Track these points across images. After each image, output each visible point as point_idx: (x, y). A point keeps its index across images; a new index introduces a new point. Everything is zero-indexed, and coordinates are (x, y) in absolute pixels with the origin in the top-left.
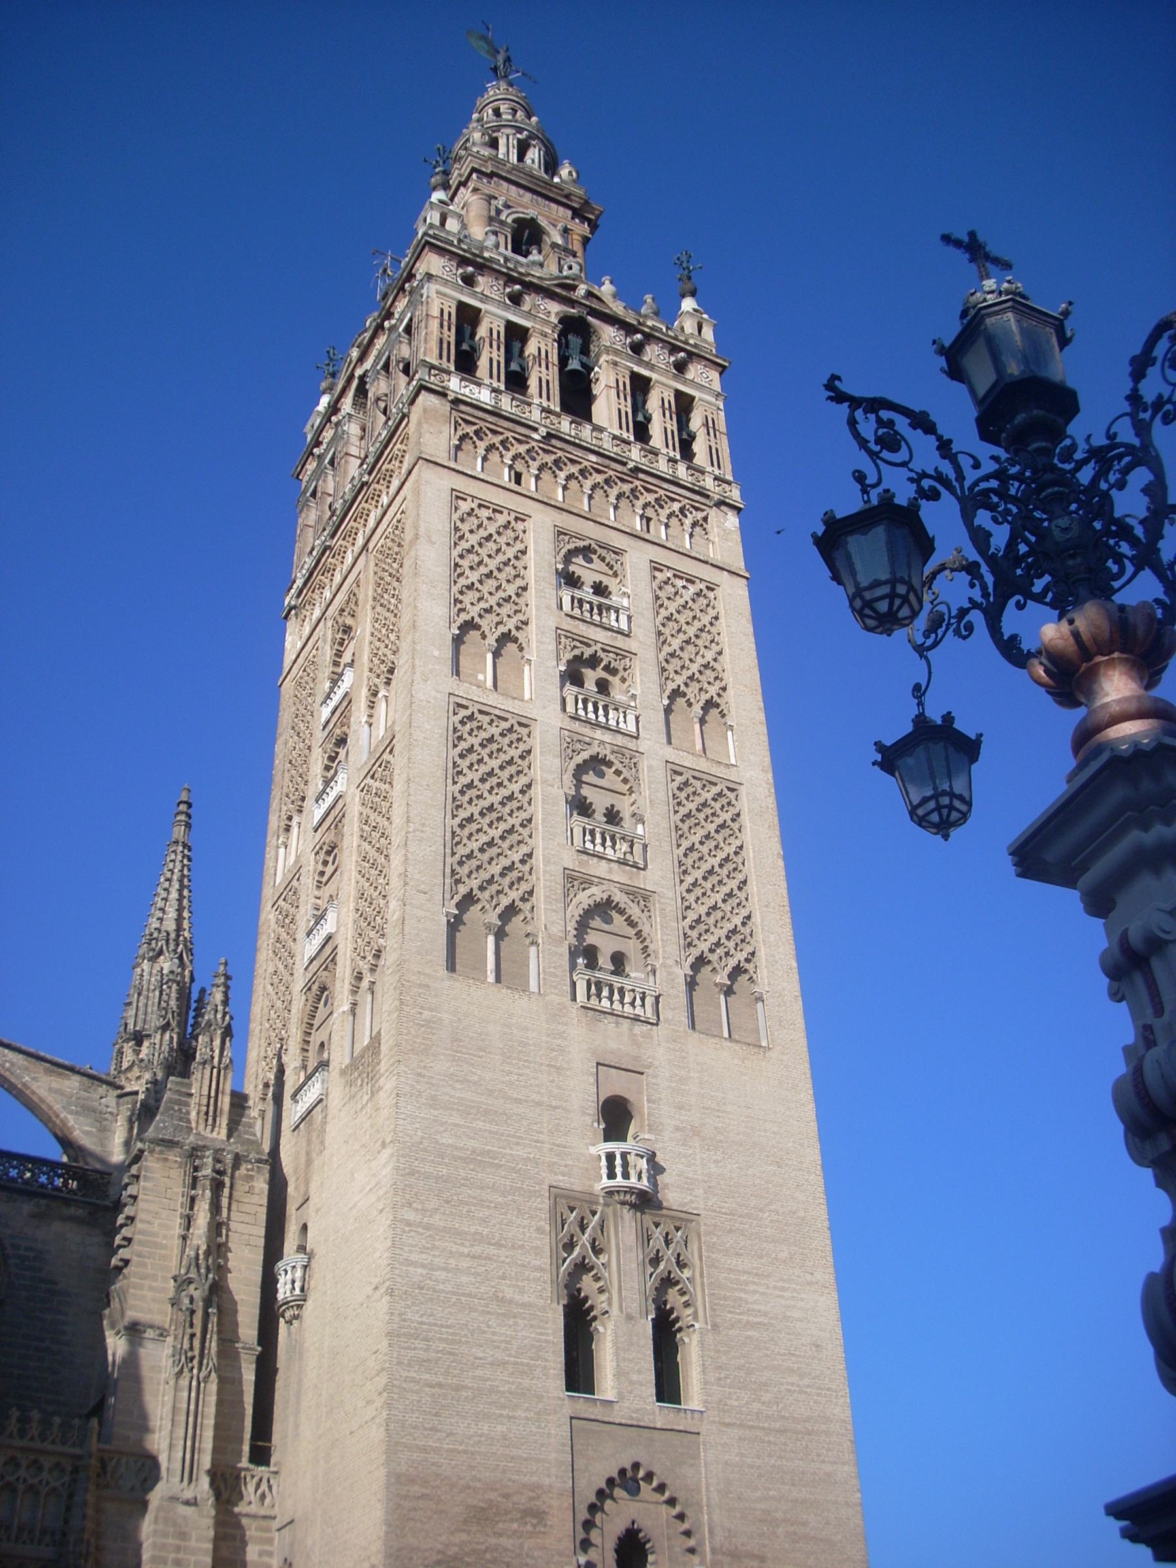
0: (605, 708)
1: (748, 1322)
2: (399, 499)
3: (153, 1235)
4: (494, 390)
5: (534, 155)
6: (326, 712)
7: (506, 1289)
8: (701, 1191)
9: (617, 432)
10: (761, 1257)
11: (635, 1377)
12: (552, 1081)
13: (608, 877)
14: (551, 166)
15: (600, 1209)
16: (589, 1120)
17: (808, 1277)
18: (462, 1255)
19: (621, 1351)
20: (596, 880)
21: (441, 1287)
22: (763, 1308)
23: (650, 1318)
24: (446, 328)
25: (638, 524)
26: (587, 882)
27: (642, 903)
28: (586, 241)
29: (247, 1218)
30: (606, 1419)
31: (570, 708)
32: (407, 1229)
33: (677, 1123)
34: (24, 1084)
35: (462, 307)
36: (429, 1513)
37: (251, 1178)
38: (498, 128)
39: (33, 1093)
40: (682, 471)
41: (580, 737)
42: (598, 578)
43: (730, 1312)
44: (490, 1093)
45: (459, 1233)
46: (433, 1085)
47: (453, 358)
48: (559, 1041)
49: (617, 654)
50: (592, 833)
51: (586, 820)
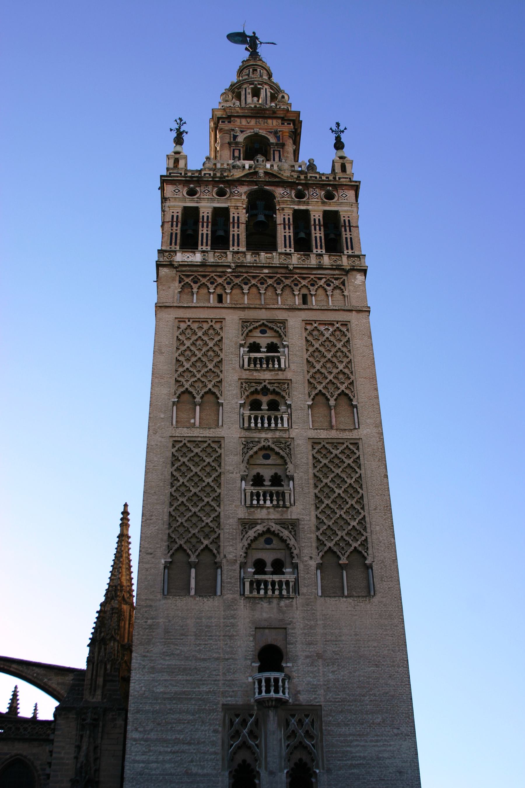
1: (351, 764)
4: (203, 252)
8: (322, 691)
10: (362, 724)
12: (227, 644)
16: (249, 662)
17: (395, 731)
18: (166, 752)
20: (259, 521)
21: (154, 772)
23: (285, 771)
24: (175, 226)
25: (298, 301)
26: (253, 524)
32: (134, 743)
33: (308, 653)
34: (45, 683)
39: (50, 687)
40: (326, 260)
41: (252, 440)
42: (269, 341)
44: (187, 658)
46: (152, 660)
47: (178, 241)
49: (279, 383)
50: (258, 495)
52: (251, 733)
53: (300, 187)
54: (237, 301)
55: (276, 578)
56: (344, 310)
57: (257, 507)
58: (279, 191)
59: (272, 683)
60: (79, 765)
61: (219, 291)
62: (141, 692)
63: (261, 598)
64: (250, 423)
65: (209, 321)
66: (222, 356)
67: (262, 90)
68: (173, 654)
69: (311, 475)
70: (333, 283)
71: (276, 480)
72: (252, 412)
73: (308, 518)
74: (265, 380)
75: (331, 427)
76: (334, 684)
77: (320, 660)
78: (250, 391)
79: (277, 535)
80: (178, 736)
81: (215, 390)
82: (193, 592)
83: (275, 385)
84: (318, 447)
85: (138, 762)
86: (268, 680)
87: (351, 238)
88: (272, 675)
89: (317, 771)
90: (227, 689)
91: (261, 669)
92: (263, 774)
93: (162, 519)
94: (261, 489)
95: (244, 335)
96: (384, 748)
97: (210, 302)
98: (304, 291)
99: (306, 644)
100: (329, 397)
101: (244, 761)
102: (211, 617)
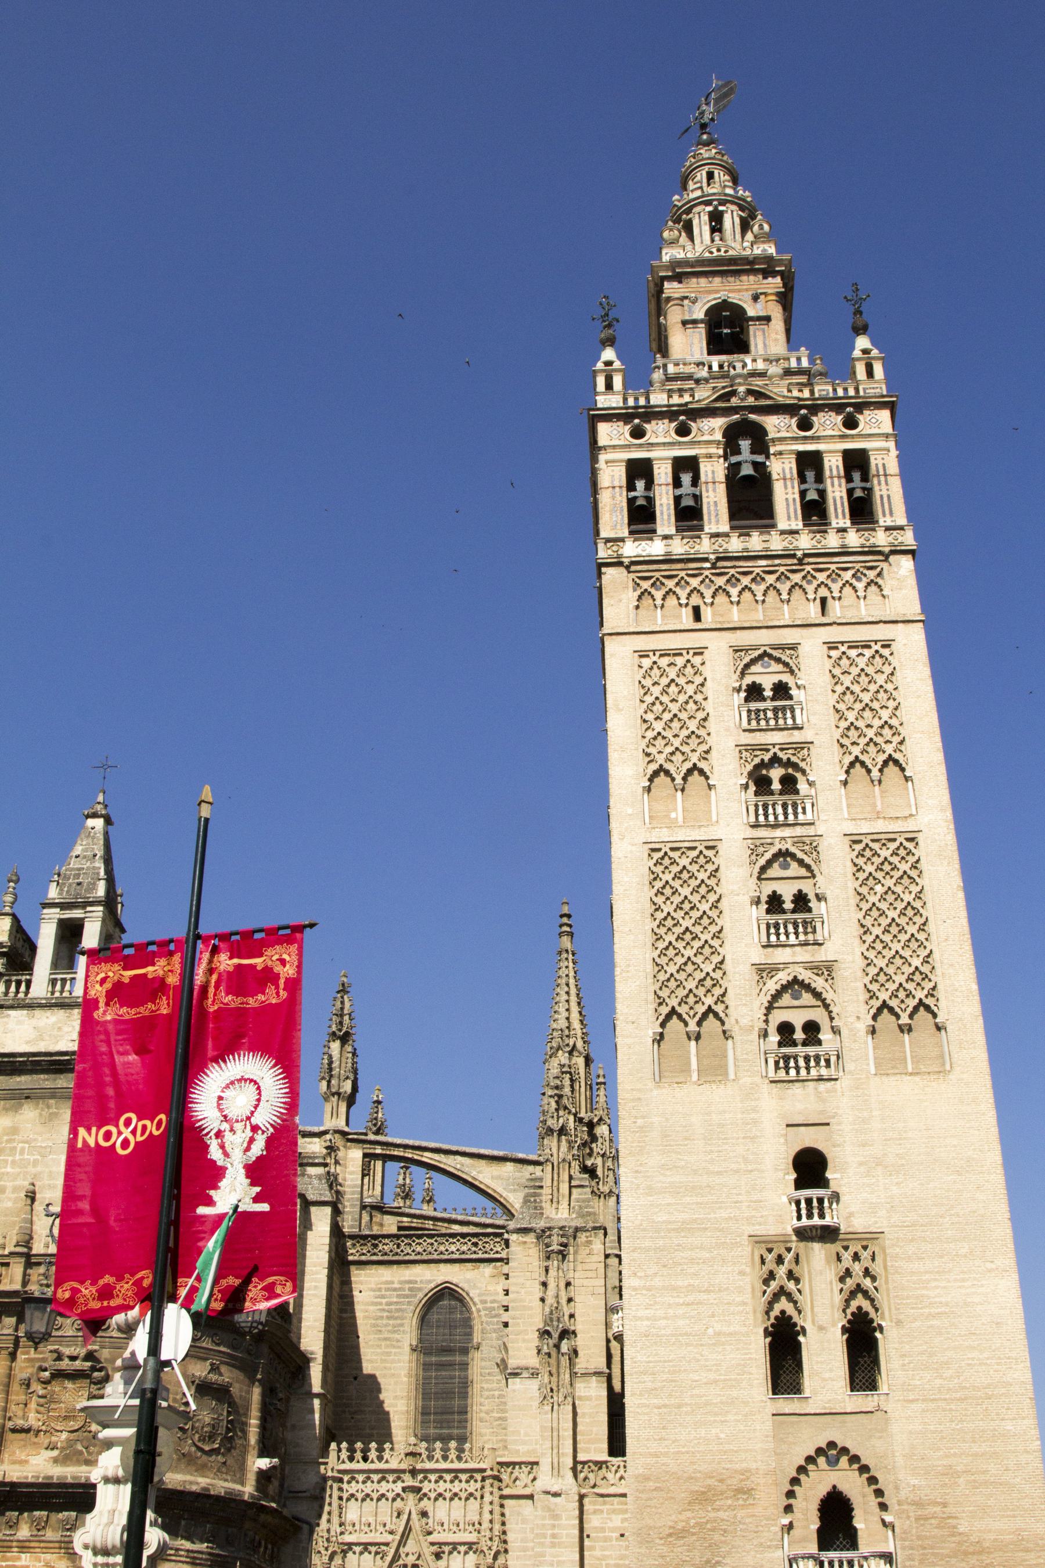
1: (930, 1314)
4: (666, 537)
7: (715, 1324)
8: (884, 1212)
10: (942, 1257)
11: (827, 1375)
13: (793, 959)
15: (793, 1245)
16: (781, 1174)
17: (989, 1265)
18: (678, 1304)
19: (824, 1354)
21: (663, 1332)
22: (943, 1300)
23: (840, 1325)
25: (813, 611)
26: (772, 970)
27: (826, 973)
29: (590, 1274)
30: (802, 1412)
33: (862, 1159)
36: (661, 1501)
37: (589, 1242)
41: (763, 841)
42: (776, 678)
43: (913, 1308)
44: (695, 1172)
45: (674, 1288)
46: (648, 1177)
48: (753, 1115)
49: (795, 749)
50: (777, 926)
51: (768, 917)
52: (790, 1275)
53: (803, 412)
54: (722, 615)
55: (811, 1050)
56: (885, 622)
57: (777, 946)
59: (815, 1203)
62: (637, 1222)
63: (792, 1081)
64: (757, 815)
65: (684, 652)
67: (725, 215)
68: (676, 1167)
69: (852, 892)
70: (865, 575)
71: (801, 901)
72: (760, 798)
73: (850, 958)
74: (774, 745)
76: (901, 1202)
77: (879, 1168)
78: (753, 763)
79: (808, 987)
80: (692, 1282)
82: (695, 1076)
83: (790, 751)
84: (858, 847)
85: (641, 1319)
86: (809, 1201)
87: (889, 497)
88: (814, 1193)
89: (883, 1324)
90: (753, 1213)
93: (644, 971)
94: (780, 918)
95: (738, 673)
96: (973, 1290)
97: (681, 622)
98: (823, 592)
99: (859, 1146)
100: (870, 766)
102: (725, 1112)
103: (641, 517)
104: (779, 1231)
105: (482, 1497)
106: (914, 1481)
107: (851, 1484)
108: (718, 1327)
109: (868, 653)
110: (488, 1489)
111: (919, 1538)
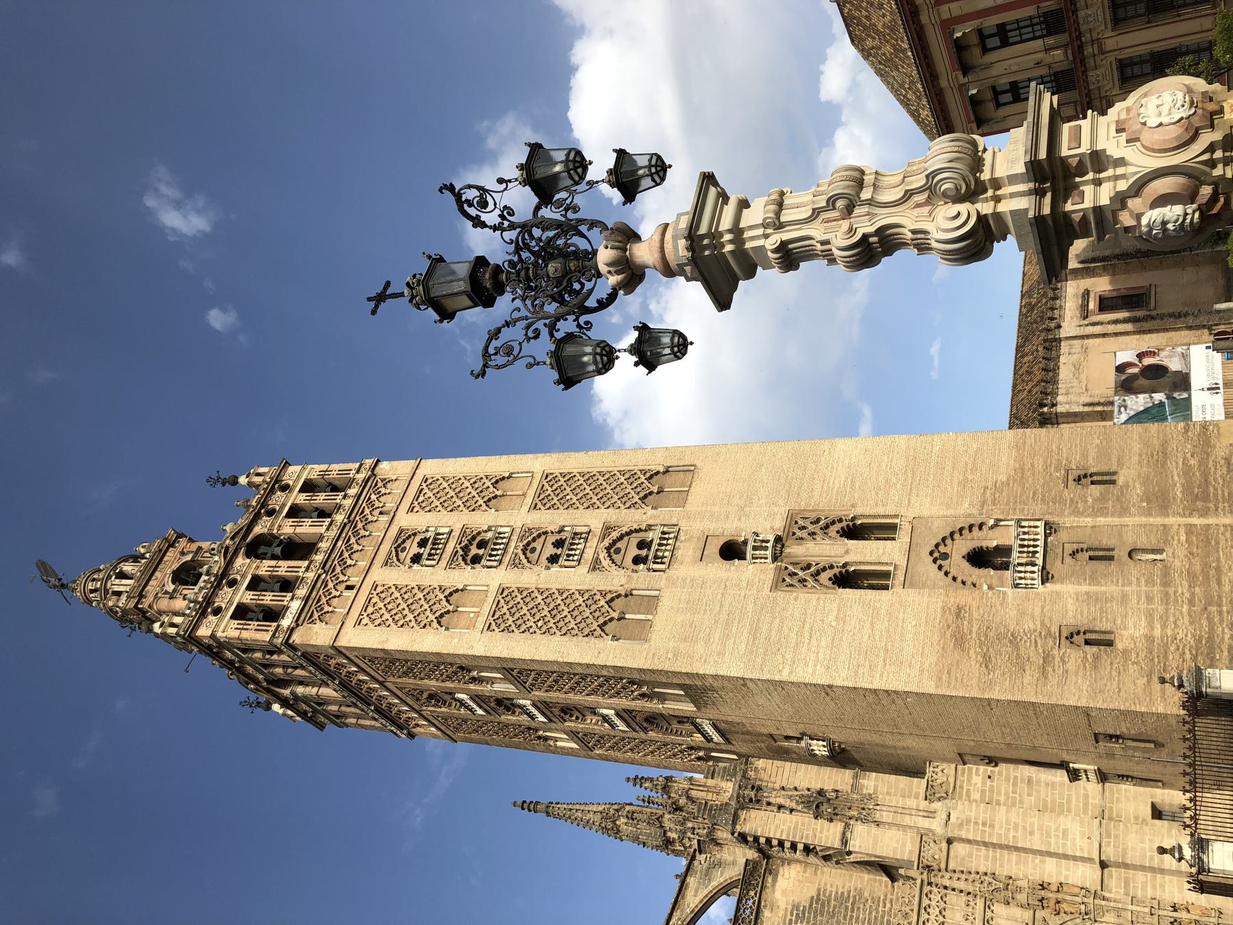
0: (495, 544)
2: (356, 660)
3: (789, 828)
5: (128, 568)
6: (480, 712)
9: (325, 528)
14: (136, 558)
25: (384, 518)
28: (191, 540)
31: (495, 564)
35: (233, 617)
38: (106, 591)
40: (352, 491)
42: (415, 544)
44: (716, 622)
50: (569, 555)
58: (258, 530)
60: (800, 808)
61: (343, 586)
66: (414, 584)
75: (524, 495)
79: (615, 542)
81: (447, 593)
82: (650, 617)
84: (539, 505)
85: (814, 671)
86: (755, 548)
91: (744, 559)
92: (847, 559)
98: (376, 512)
101: (830, 579)
103: (272, 615)
104: (772, 572)
105: (946, 888)
106: (967, 505)
107: (962, 547)
108: (832, 618)
109: (426, 490)
110: (939, 881)
111: (1008, 504)
